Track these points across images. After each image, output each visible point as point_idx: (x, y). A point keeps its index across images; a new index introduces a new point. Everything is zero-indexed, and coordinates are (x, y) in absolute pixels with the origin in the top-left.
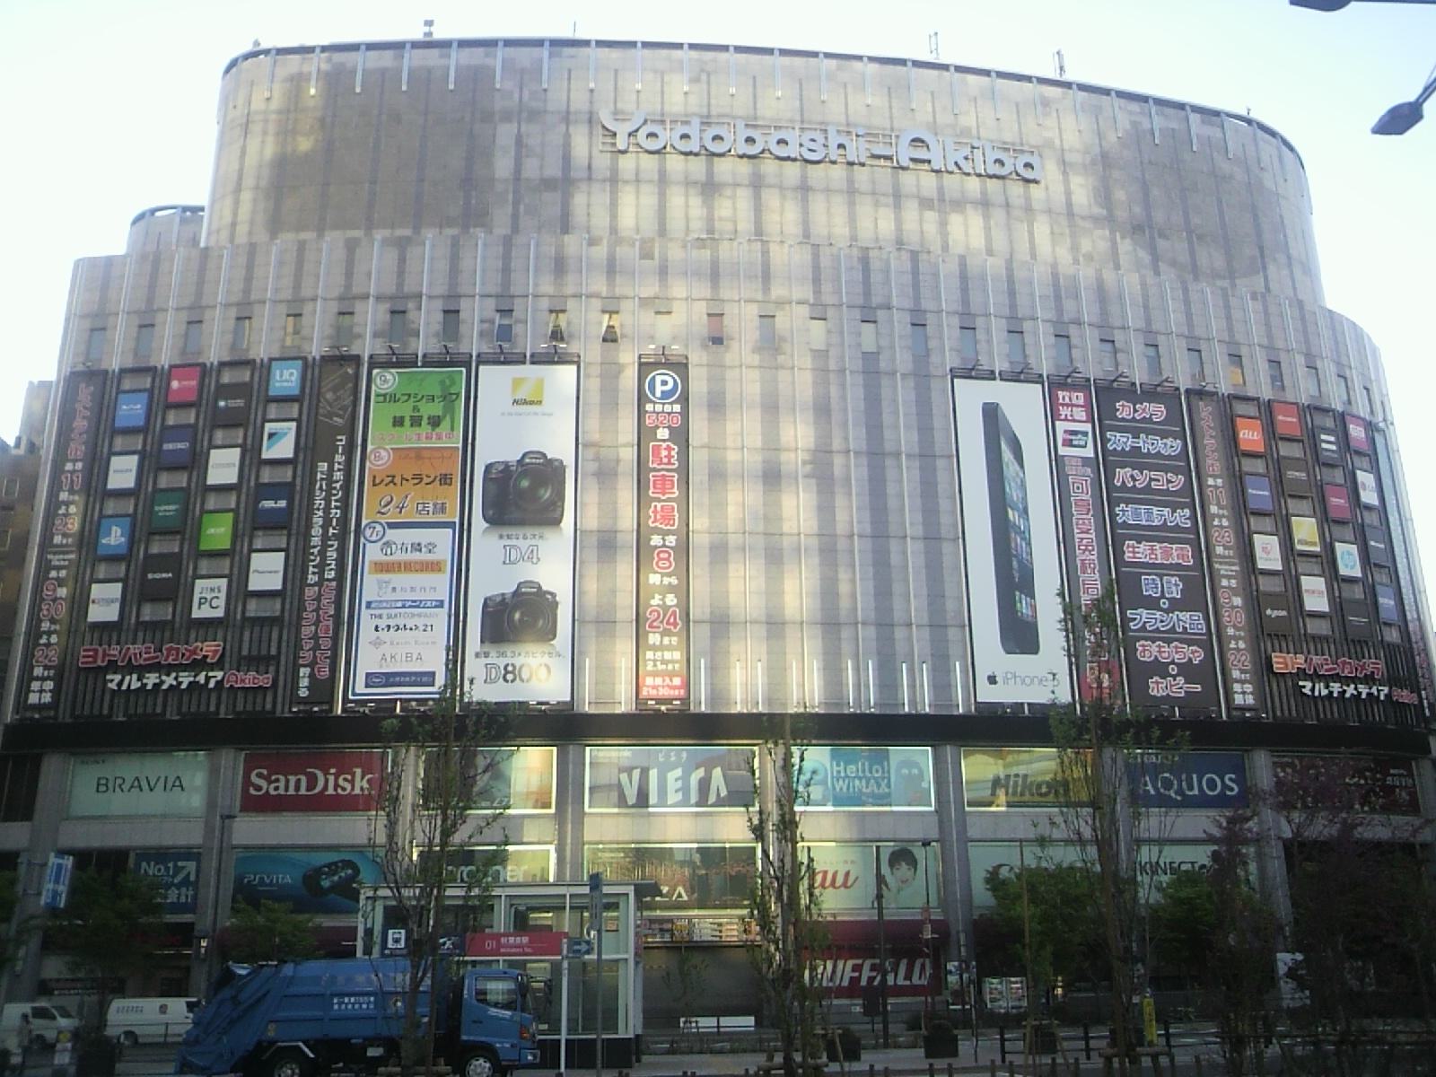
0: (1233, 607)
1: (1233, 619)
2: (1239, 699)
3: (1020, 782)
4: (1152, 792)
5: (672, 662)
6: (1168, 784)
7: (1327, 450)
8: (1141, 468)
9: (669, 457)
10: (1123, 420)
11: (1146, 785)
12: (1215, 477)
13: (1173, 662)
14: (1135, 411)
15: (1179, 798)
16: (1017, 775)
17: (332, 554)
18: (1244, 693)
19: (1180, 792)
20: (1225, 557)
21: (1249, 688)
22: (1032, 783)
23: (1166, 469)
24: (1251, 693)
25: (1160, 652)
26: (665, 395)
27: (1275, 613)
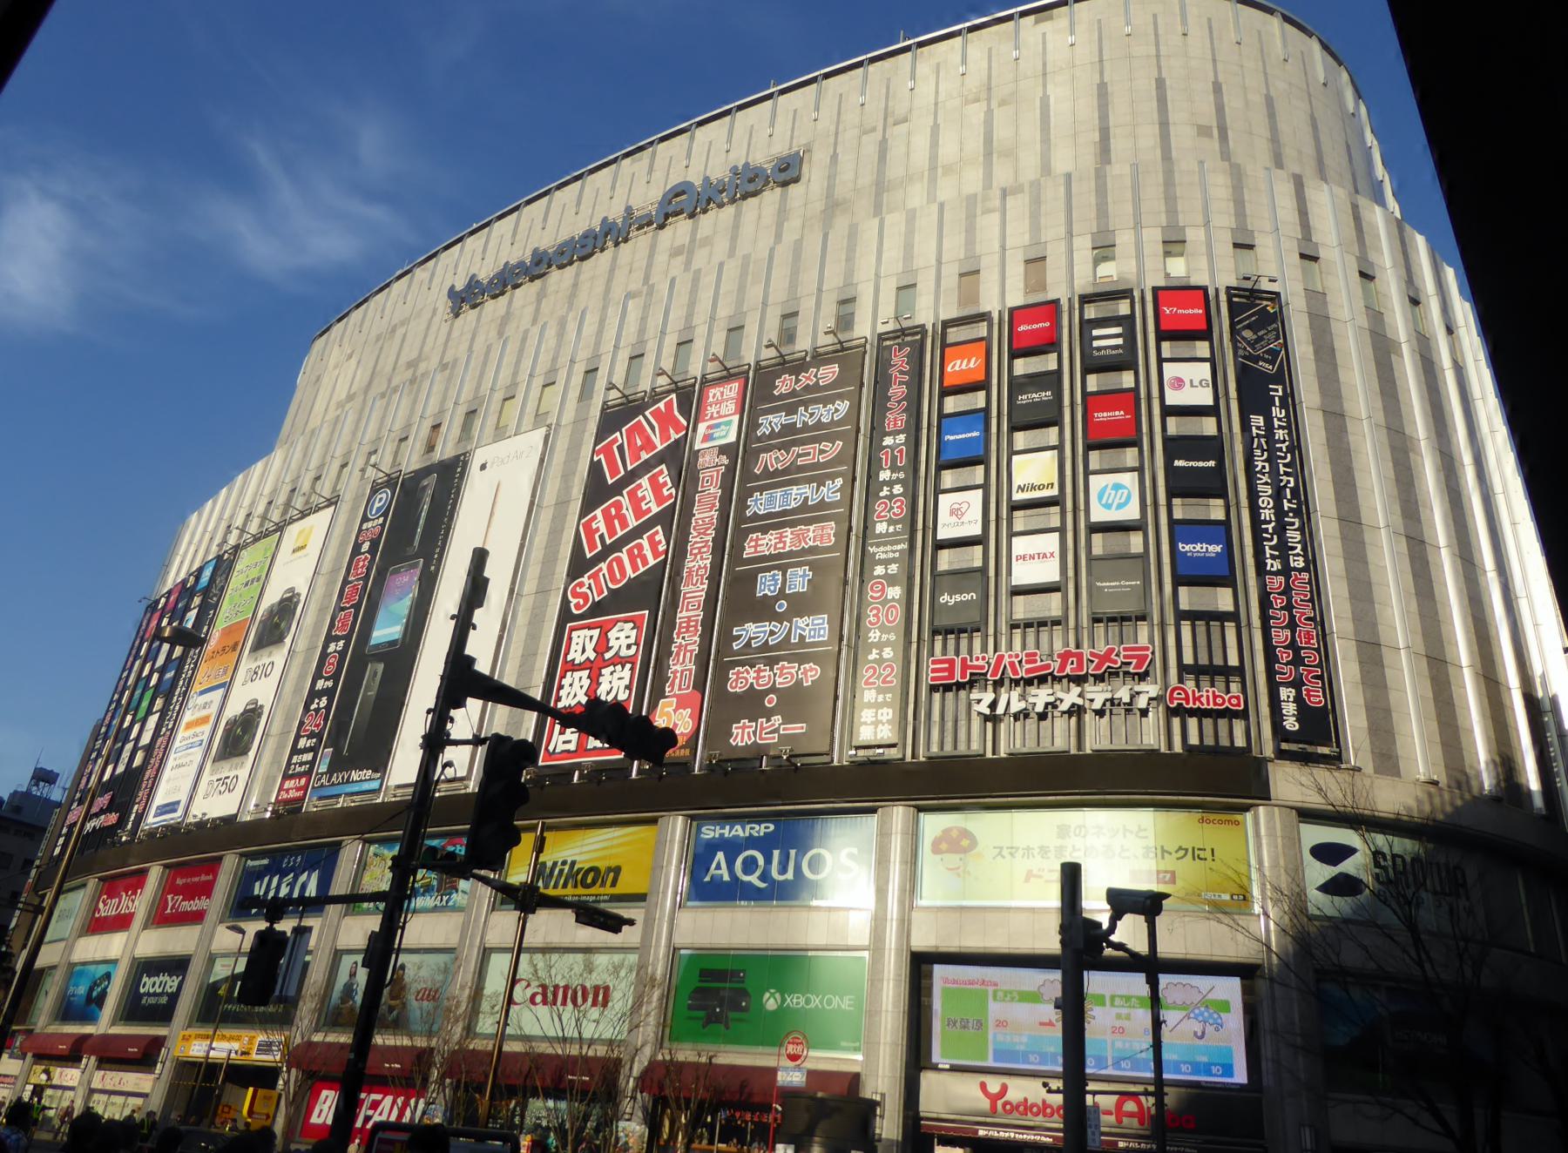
0: (886, 601)
2: (865, 734)
3: (566, 871)
4: (726, 878)
5: (305, 763)
6: (750, 866)
7: (1099, 349)
9: (362, 567)
11: (718, 867)
12: (895, 433)
13: (773, 690)
15: (762, 885)
16: (564, 863)
17: (177, 708)
18: (876, 723)
19: (764, 877)
20: (887, 534)
21: (887, 714)
22: (580, 870)
26: (379, 509)
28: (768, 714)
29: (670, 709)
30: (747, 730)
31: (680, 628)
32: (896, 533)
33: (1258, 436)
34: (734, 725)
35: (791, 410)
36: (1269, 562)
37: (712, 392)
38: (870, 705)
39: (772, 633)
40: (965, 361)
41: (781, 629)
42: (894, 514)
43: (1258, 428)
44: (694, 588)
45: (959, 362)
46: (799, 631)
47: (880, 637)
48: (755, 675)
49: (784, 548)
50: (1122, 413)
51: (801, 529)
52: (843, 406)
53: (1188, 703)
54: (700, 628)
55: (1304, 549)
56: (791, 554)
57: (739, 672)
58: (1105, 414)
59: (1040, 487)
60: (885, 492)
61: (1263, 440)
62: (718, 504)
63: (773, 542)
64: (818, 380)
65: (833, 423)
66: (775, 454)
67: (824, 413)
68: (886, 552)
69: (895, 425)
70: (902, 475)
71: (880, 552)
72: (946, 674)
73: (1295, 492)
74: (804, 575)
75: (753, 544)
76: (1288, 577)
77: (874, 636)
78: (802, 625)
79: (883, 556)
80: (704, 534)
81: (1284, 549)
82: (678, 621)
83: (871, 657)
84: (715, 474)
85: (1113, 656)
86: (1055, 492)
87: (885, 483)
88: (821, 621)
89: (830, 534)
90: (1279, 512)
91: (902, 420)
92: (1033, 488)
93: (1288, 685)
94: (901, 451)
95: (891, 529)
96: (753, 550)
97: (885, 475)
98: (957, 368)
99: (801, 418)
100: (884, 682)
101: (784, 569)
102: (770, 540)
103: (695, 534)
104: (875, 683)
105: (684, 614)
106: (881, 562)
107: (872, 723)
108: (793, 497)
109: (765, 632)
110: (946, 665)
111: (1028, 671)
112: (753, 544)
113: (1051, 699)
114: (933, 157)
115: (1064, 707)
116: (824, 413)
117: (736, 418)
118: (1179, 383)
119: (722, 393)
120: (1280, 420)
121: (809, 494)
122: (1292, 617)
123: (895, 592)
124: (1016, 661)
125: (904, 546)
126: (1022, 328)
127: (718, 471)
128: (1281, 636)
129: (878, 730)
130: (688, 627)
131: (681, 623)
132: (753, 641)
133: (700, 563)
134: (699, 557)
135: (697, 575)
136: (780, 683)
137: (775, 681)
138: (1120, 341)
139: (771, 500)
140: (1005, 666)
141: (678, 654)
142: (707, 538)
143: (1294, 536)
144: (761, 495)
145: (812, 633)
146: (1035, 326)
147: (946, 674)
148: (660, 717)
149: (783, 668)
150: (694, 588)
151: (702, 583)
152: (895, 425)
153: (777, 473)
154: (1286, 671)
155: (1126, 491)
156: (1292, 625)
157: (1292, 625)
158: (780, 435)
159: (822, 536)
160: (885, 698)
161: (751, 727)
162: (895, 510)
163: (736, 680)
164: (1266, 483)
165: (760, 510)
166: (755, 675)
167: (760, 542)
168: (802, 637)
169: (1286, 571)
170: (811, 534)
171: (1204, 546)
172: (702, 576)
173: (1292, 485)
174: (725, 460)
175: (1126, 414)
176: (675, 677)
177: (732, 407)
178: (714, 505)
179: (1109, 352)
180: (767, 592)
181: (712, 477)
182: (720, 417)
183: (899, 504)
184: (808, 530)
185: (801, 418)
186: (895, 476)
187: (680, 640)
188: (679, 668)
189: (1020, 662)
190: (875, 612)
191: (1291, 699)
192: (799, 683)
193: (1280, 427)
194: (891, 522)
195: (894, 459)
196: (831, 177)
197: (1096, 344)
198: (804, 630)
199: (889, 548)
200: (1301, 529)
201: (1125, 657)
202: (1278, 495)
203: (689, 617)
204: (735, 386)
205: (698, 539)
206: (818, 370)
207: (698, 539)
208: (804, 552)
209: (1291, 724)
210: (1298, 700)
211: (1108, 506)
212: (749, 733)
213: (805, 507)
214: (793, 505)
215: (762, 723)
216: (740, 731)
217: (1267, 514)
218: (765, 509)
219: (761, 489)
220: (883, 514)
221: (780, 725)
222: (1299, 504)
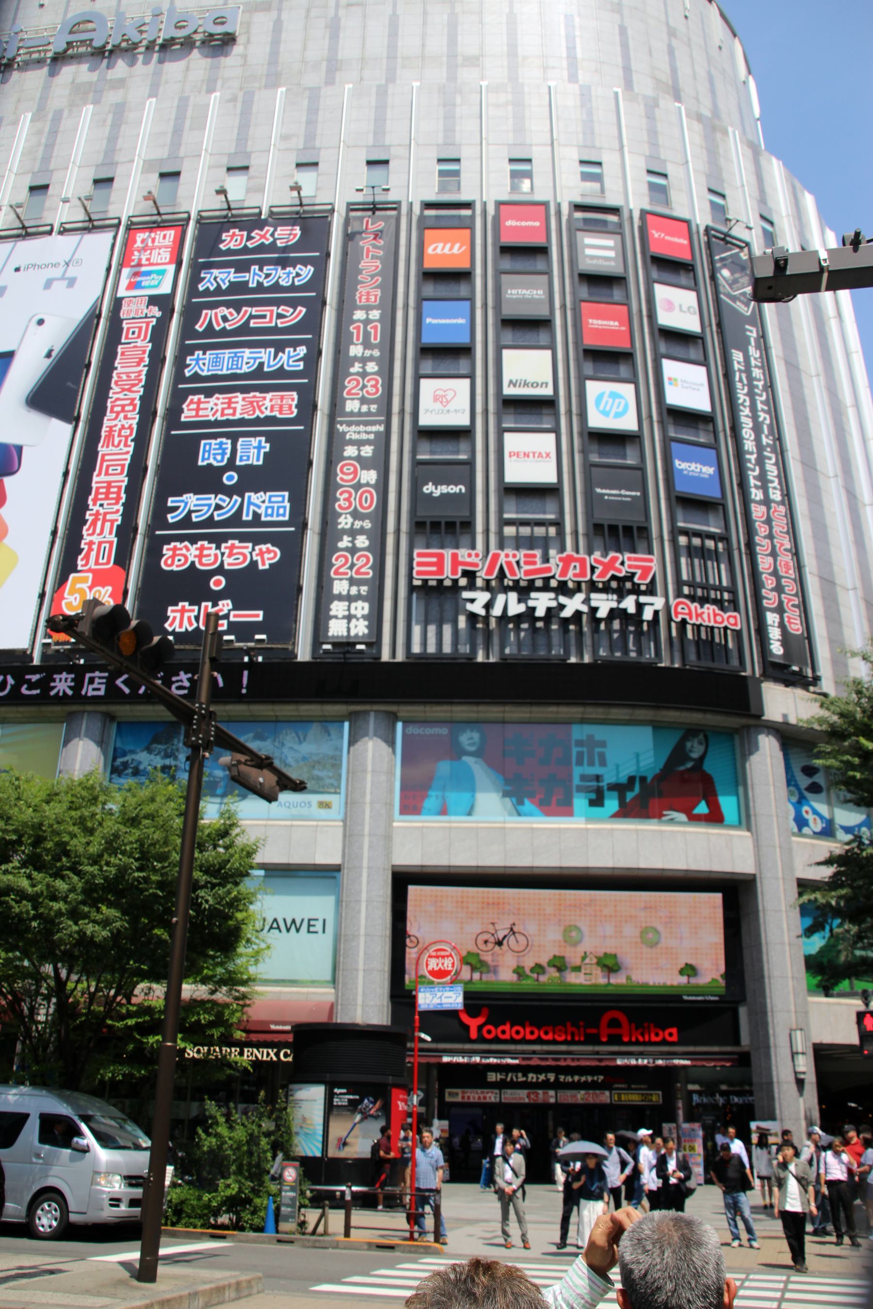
0: (358, 486)
1: (355, 503)
2: (337, 629)
8: (237, 306)
10: (230, 252)
12: (367, 308)
14: (249, 238)
20: (359, 414)
21: (362, 608)
23: (277, 302)
24: (364, 617)
25: (200, 556)
27: (444, 489)
28: (215, 598)
29: (85, 586)
30: (186, 615)
31: (97, 493)
32: (369, 413)
33: (740, 371)
34: (170, 608)
35: (242, 267)
36: (753, 491)
37: (140, 236)
38: (340, 598)
39: (218, 507)
40: (448, 246)
41: (230, 505)
42: (367, 392)
43: (739, 363)
44: (115, 450)
45: (441, 245)
46: (252, 508)
47: (353, 524)
48: (197, 553)
49: (234, 414)
50: (616, 323)
51: (254, 397)
52: (307, 272)
53: (691, 618)
54: (123, 496)
55: (780, 483)
56: (242, 422)
57: (175, 549)
58: (600, 322)
59: (535, 385)
60: (356, 368)
61: (744, 376)
62: (147, 360)
63: (220, 407)
64: (275, 240)
65: (293, 288)
66: (223, 311)
67: (284, 276)
68: (359, 433)
69: (368, 300)
70: (376, 353)
71: (352, 432)
72: (434, 569)
73: (770, 426)
74: (259, 447)
75: (194, 406)
76: (769, 508)
77: (345, 522)
78: (258, 502)
79: (355, 437)
80: (129, 390)
81: (763, 477)
82: (94, 485)
83: (341, 545)
84: (144, 325)
85: (617, 565)
86: (548, 391)
87: (356, 359)
88: (280, 499)
89: (290, 406)
90: (760, 447)
91: (376, 296)
92: (526, 384)
93: (773, 610)
94: (375, 328)
95: (365, 408)
96: (194, 413)
97: (356, 350)
98: (439, 251)
99: (253, 277)
100: (357, 573)
101: (234, 438)
102: (216, 404)
103: (117, 389)
104: (346, 574)
105: (103, 478)
106: (352, 442)
107: (344, 617)
108: (245, 360)
109: (210, 506)
110: (434, 560)
111: (527, 573)
112: (194, 406)
113: (554, 604)
114: (392, 47)
115: (567, 613)
116: (284, 276)
117: (172, 268)
118: (670, 306)
119: (153, 240)
120: (755, 359)
121: (265, 359)
122: (773, 547)
123: (370, 476)
124: (513, 561)
125: (381, 428)
126: (509, 223)
127: (148, 324)
128: (764, 563)
129: (352, 625)
130: (107, 494)
131: (98, 489)
132: (193, 515)
133: (124, 422)
134: (122, 415)
135: (119, 435)
136: (229, 564)
137: (222, 562)
138: (612, 254)
139: (217, 361)
140: (501, 568)
141: (94, 523)
142: (132, 395)
143: (772, 471)
144: (204, 354)
145: (270, 511)
146: (524, 224)
147: (434, 569)
148: (70, 594)
149: (233, 547)
150: (115, 450)
151: (126, 445)
152: (368, 300)
153: (224, 333)
154: (770, 599)
155: (623, 402)
156: (774, 554)
157: (774, 554)
158: (228, 291)
159: (281, 407)
160: (359, 591)
161: (193, 611)
162: (369, 389)
163: (173, 557)
164: (747, 416)
165: (203, 370)
166: (197, 553)
167: (202, 406)
168: (256, 515)
169: (767, 502)
170: (268, 403)
171: (699, 466)
172: (127, 437)
173: (768, 422)
174: (156, 312)
175: (621, 325)
176: (90, 550)
177: (166, 256)
178: (142, 360)
179: (601, 262)
180: (212, 461)
181: (140, 328)
182: (151, 264)
183: (373, 382)
184: (264, 398)
185: (253, 277)
186: (368, 353)
187: (97, 508)
188: (95, 539)
189: (518, 563)
190: (346, 495)
191: (776, 624)
192: (254, 564)
193: (756, 366)
194: (363, 401)
195: (367, 334)
196: (276, 42)
197: (588, 252)
198: (259, 507)
199: (362, 428)
200: (776, 464)
201: (630, 566)
202: (757, 429)
203: (109, 483)
204: (171, 234)
205: (121, 396)
206: (275, 230)
207: (121, 396)
208: (257, 422)
209: (777, 649)
210: (782, 626)
211: (606, 414)
212: (189, 618)
213: (259, 372)
214: (245, 369)
215: (206, 607)
216: (178, 615)
217: (749, 445)
218: (209, 370)
219: (205, 348)
220: (354, 391)
221: (229, 611)
222: (774, 440)
